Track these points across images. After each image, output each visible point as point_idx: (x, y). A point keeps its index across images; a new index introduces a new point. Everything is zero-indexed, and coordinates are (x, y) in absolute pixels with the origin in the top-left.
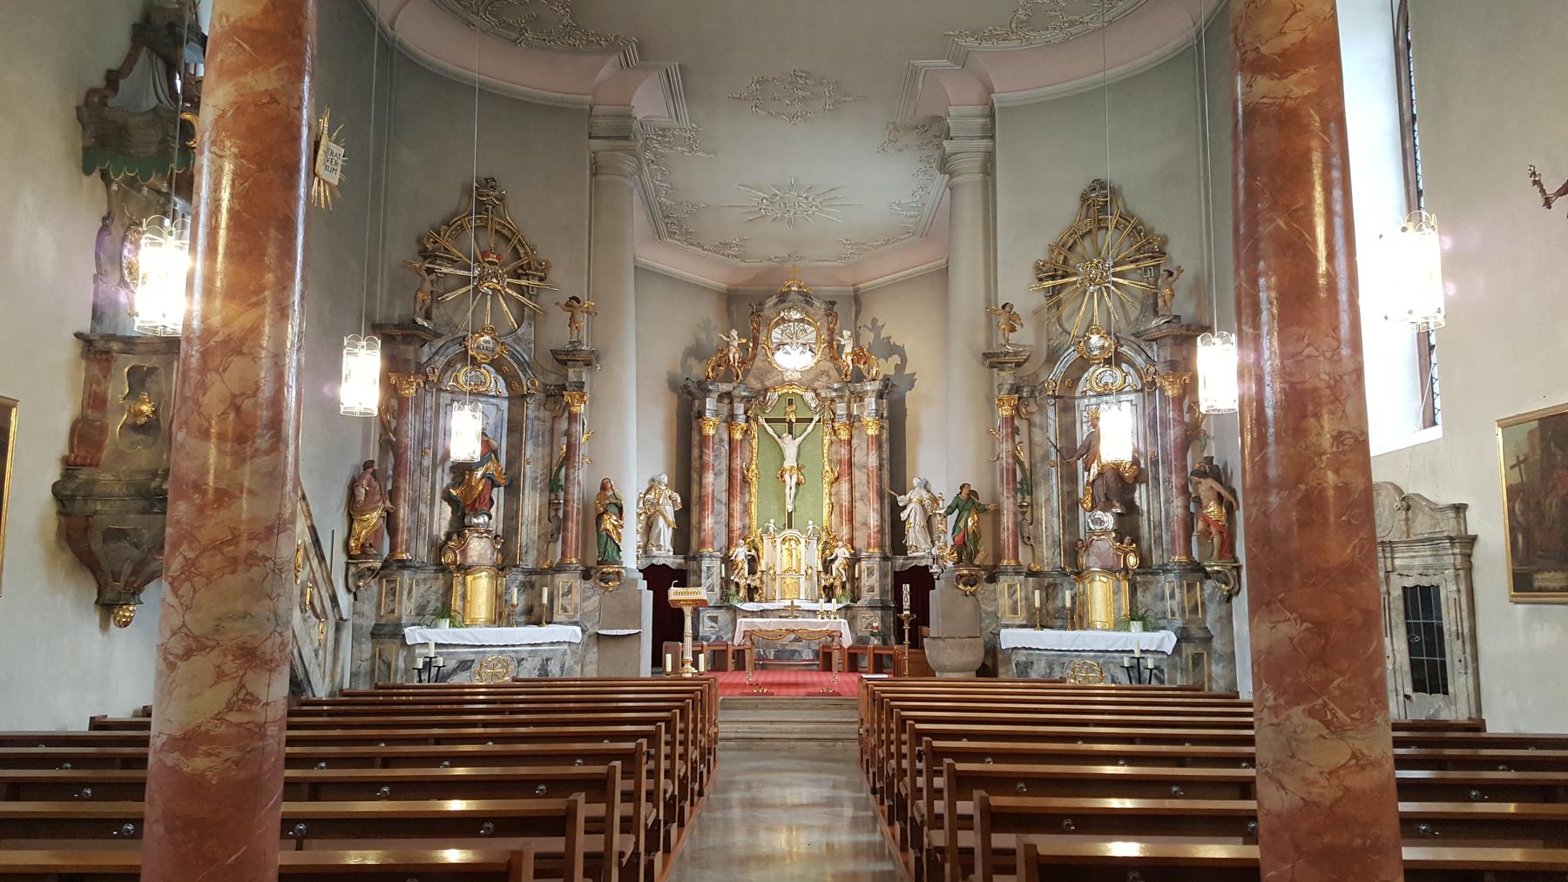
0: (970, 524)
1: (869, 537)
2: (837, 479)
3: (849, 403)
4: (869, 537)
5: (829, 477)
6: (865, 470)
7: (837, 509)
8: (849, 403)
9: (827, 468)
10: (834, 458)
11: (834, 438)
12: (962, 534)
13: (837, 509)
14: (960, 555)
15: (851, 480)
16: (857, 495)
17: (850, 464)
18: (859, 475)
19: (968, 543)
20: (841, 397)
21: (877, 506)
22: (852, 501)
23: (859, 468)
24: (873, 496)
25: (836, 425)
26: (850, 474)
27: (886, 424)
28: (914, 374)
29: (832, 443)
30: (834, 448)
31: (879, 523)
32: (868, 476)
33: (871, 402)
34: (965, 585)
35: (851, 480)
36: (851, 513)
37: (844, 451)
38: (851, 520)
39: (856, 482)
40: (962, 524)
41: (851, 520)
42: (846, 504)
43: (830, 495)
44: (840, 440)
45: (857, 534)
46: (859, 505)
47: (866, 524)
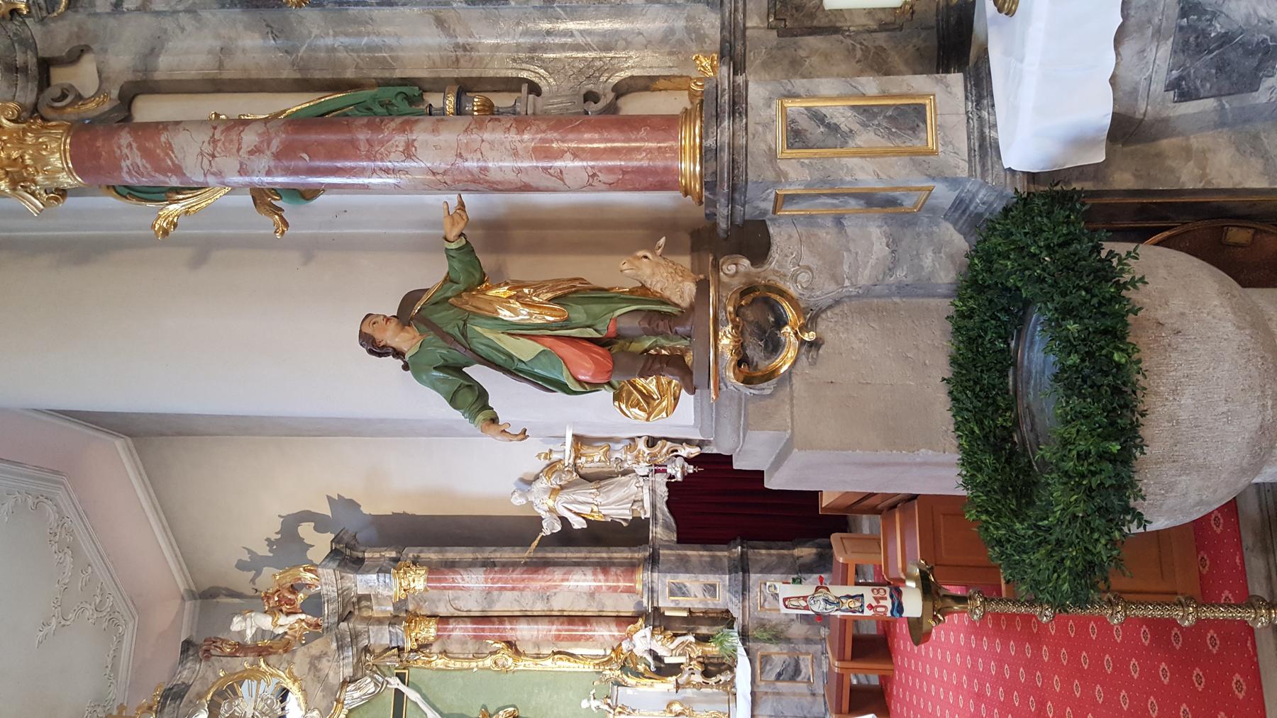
0: (523, 315)
1: (615, 589)
2: (510, 644)
3: (369, 620)
4: (615, 589)
5: (506, 659)
6: (496, 593)
7: (564, 646)
8: (369, 620)
9: (488, 662)
10: (472, 647)
11: (435, 649)
12: (566, 350)
13: (564, 646)
14: (652, 364)
15: (513, 618)
16: (539, 607)
17: (484, 619)
18: (505, 603)
19: (603, 329)
20: (355, 636)
21: (558, 574)
22: (549, 617)
23: (491, 603)
24: (540, 581)
25: (409, 645)
26: (501, 619)
27: (411, 553)
28: (329, 498)
29: (444, 653)
30: (454, 648)
31: (589, 571)
32: (501, 589)
33: (364, 583)
34: (774, 347)
35: (513, 618)
36: (571, 619)
37: (459, 631)
38: (584, 620)
39: (515, 609)
40: (524, 350)
41: (584, 620)
42: (554, 629)
43: (538, 656)
44: (438, 637)
45: (610, 609)
46: (560, 604)
47: (592, 595)
